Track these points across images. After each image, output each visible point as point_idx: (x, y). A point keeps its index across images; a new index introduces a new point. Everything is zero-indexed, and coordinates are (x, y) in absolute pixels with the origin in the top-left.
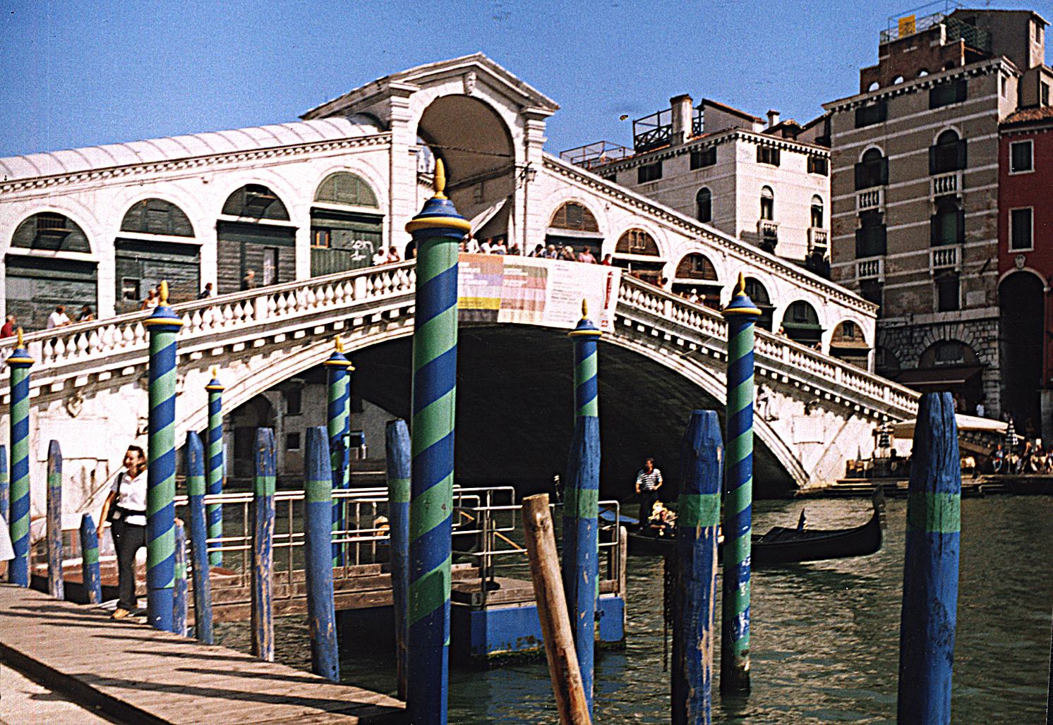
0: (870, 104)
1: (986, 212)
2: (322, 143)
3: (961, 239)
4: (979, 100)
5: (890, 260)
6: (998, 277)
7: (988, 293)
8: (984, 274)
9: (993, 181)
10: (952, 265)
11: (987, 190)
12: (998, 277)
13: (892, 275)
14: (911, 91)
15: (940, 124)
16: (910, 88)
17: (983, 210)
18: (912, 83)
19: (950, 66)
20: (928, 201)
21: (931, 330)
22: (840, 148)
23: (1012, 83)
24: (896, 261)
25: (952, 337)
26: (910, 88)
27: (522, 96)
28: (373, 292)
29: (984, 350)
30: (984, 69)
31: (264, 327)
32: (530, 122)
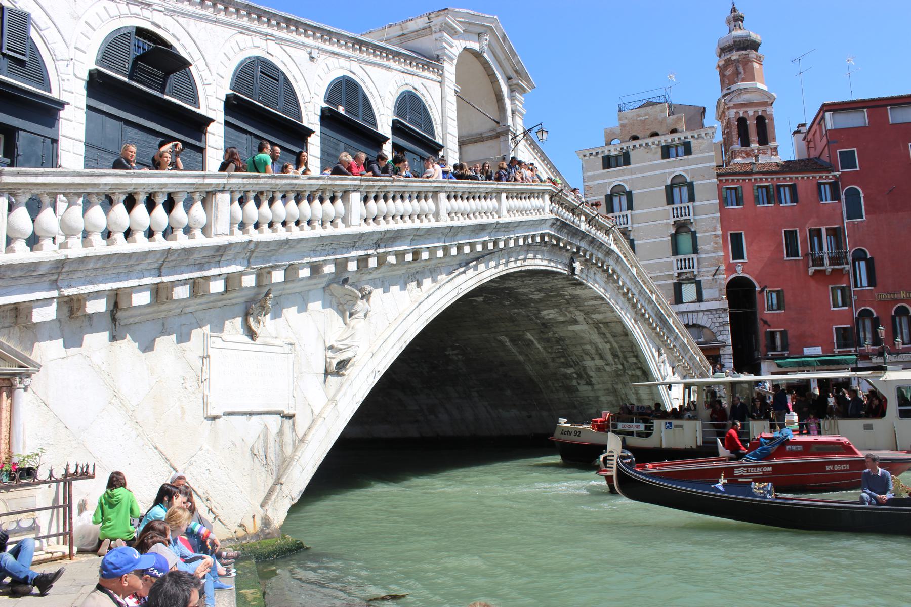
0: (613, 153)
3: (695, 250)
4: (700, 155)
10: (691, 270)
15: (672, 170)
16: (647, 144)
19: (674, 131)
20: (667, 224)
22: (591, 183)
26: (647, 144)
30: (703, 135)
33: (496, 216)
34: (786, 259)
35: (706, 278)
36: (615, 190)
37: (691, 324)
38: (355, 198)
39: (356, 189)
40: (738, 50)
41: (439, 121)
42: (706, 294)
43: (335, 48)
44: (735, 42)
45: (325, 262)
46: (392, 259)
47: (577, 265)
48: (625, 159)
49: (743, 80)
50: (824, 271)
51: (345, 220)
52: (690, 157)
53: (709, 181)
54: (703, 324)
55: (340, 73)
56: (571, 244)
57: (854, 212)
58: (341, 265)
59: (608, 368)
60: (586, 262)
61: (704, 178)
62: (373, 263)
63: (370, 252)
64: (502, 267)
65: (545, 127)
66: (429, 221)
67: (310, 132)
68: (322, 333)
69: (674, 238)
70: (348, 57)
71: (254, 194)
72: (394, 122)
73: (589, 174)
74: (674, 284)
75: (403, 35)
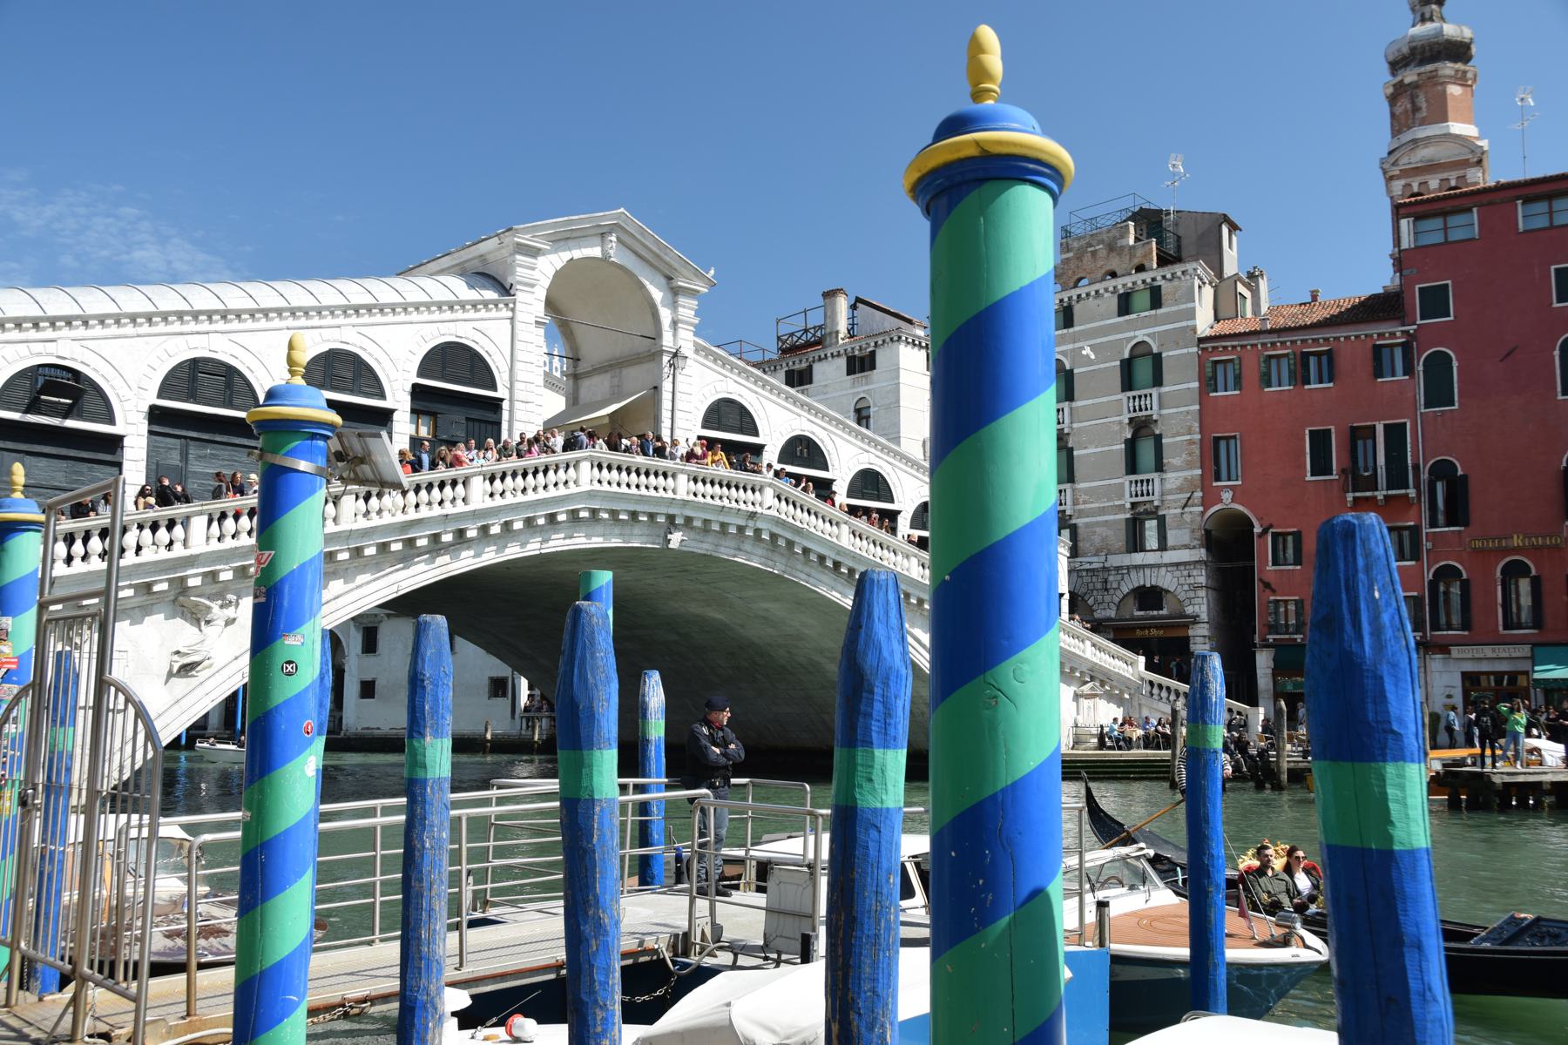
2: (428, 306)
3: (1159, 467)
4: (1174, 308)
6: (1203, 513)
15: (1131, 334)
18: (1100, 286)
19: (1140, 268)
20: (1120, 422)
23: (1208, 292)
24: (1087, 491)
28: (492, 495)
31: (350, 534)
34: (1309, 478)
40: (1422, 62)
41: (505, 368)
44: (1413, 49)
45: (156, 582)
49: (1423, 122)
52: (1160, 311)
55: (324, 348)
57: (1438, 393)
61: (1177, 346)
69: (1131, 446)
72: (415, 386)
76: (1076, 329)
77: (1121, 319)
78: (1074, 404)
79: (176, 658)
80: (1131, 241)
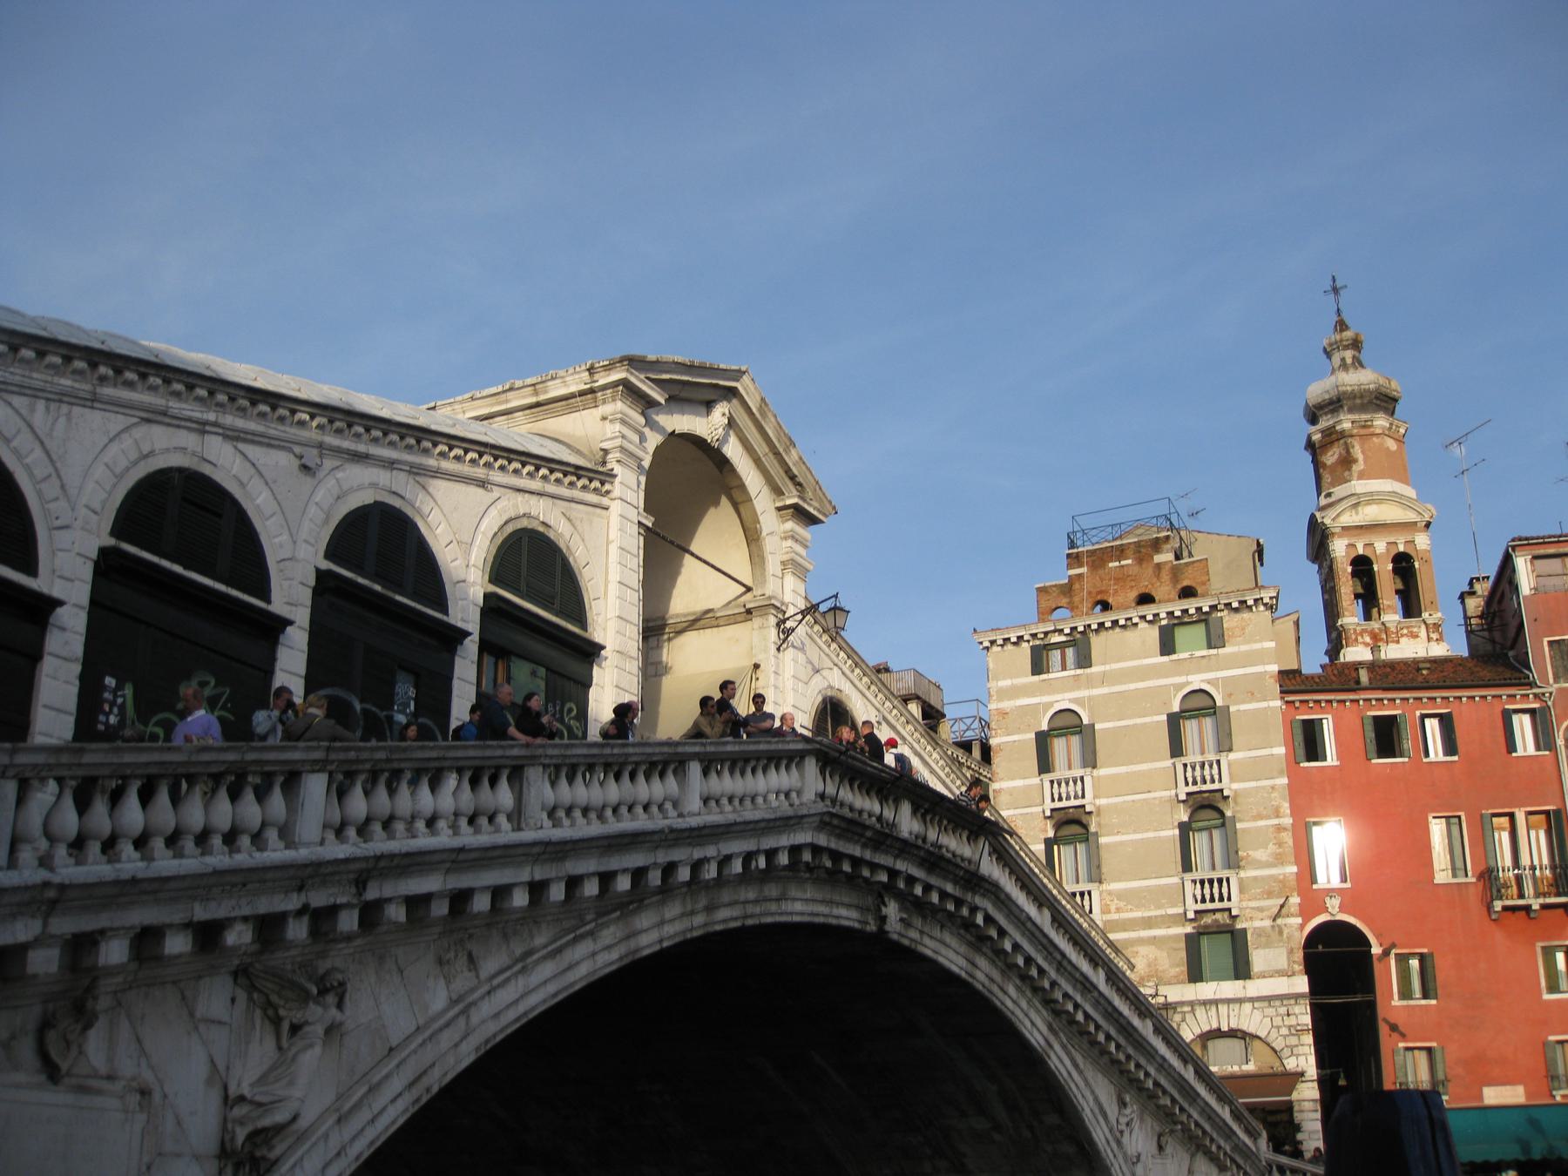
1: (1276, 821)
3: (1233, 861)
4: (1244, 648)
5: (1110, 893)
6: (1302, 927)
7: (1291, 952)
8: (1279, 921)
9: (1280, 774)
10: (1225, 904)
11: (1273, 788)
12: (1302, 927)
13: (1115, 916)
14: (1130, 625)
15: (1182, 679)
17: (1268, 817)
18: (1134, 614)
19: (1188, 593)
21: (1193, 1011)
22: (1006, 705)
24: (1121, 895)
25: (1233, 1025)
27: (788, 471)
29: (1292, 1047)
32: (790, 525)
33: (672, 813)
35: (1257, 924)
36: (1059, 723)
37: (1225, 1028)
38: (315, 786)
39: (319, 766)
42: (1259, 959)
43: (362, 448)
46: (397, 913)
47: (892, 910)
48: (1080, 648)
49: (1361, 476)
50: (1527, 908)
51: (286, 833)
53: (1264, 704)
54: (1252, 1030)
55: (366, 498)
56: (874, 867)
58: (269, 928)
59: (997, 1137)
60: (917, 907)
61: (1252, 696)
62: (348, 921)
63: (341, 900)
64: (699, 920)
65: (843, 602)
66: (498, 830)
67: (279, 625)
68: (221, 1066)
69: (1185, 829)
70: (391, 465)
71: (73, 783)
72: (487, 596)
73: (1002, 683)
74: (1187, 935)
75: (538, 405)
76: (1093, 669)
77: (1166, 658)
78: (1095, 772)
79: (238, 1111)
80: (1170, 557)
